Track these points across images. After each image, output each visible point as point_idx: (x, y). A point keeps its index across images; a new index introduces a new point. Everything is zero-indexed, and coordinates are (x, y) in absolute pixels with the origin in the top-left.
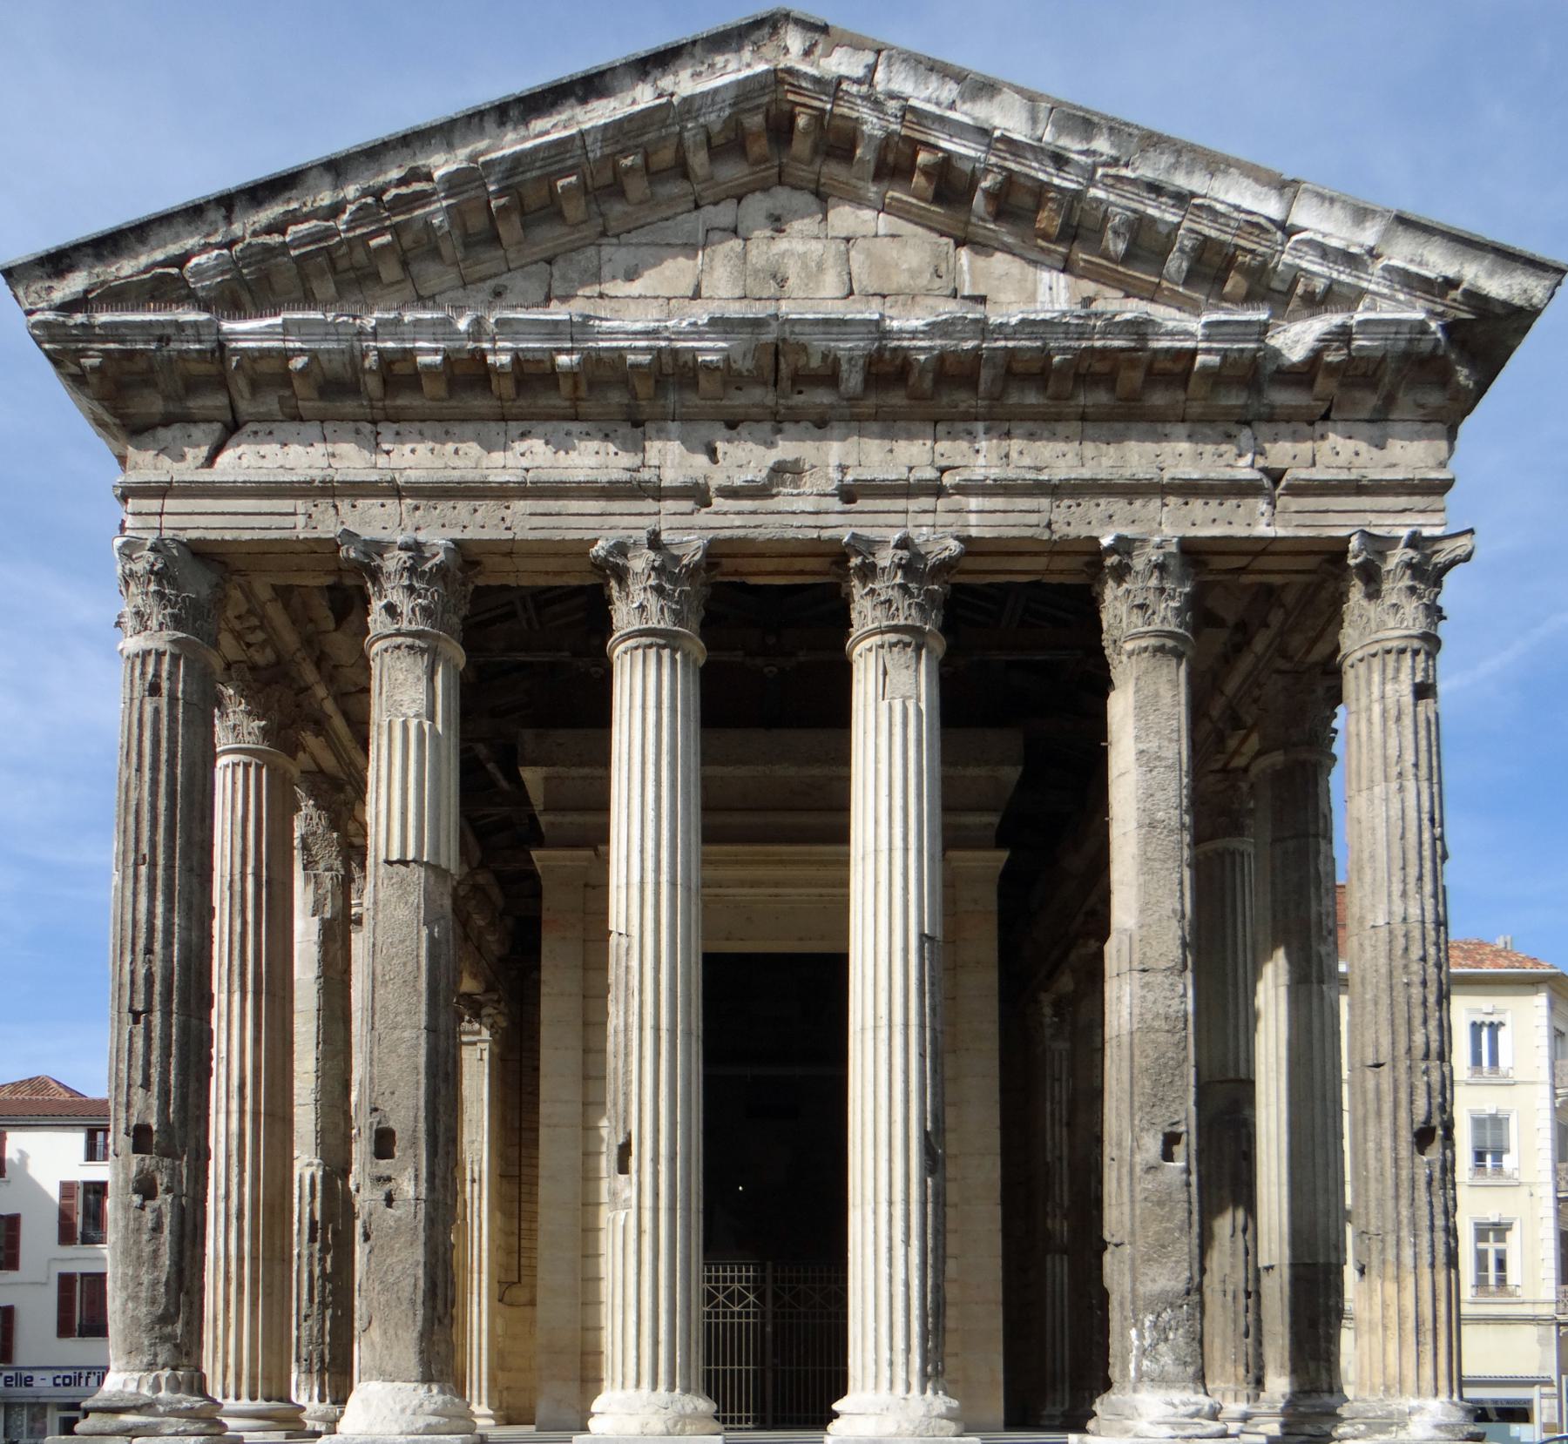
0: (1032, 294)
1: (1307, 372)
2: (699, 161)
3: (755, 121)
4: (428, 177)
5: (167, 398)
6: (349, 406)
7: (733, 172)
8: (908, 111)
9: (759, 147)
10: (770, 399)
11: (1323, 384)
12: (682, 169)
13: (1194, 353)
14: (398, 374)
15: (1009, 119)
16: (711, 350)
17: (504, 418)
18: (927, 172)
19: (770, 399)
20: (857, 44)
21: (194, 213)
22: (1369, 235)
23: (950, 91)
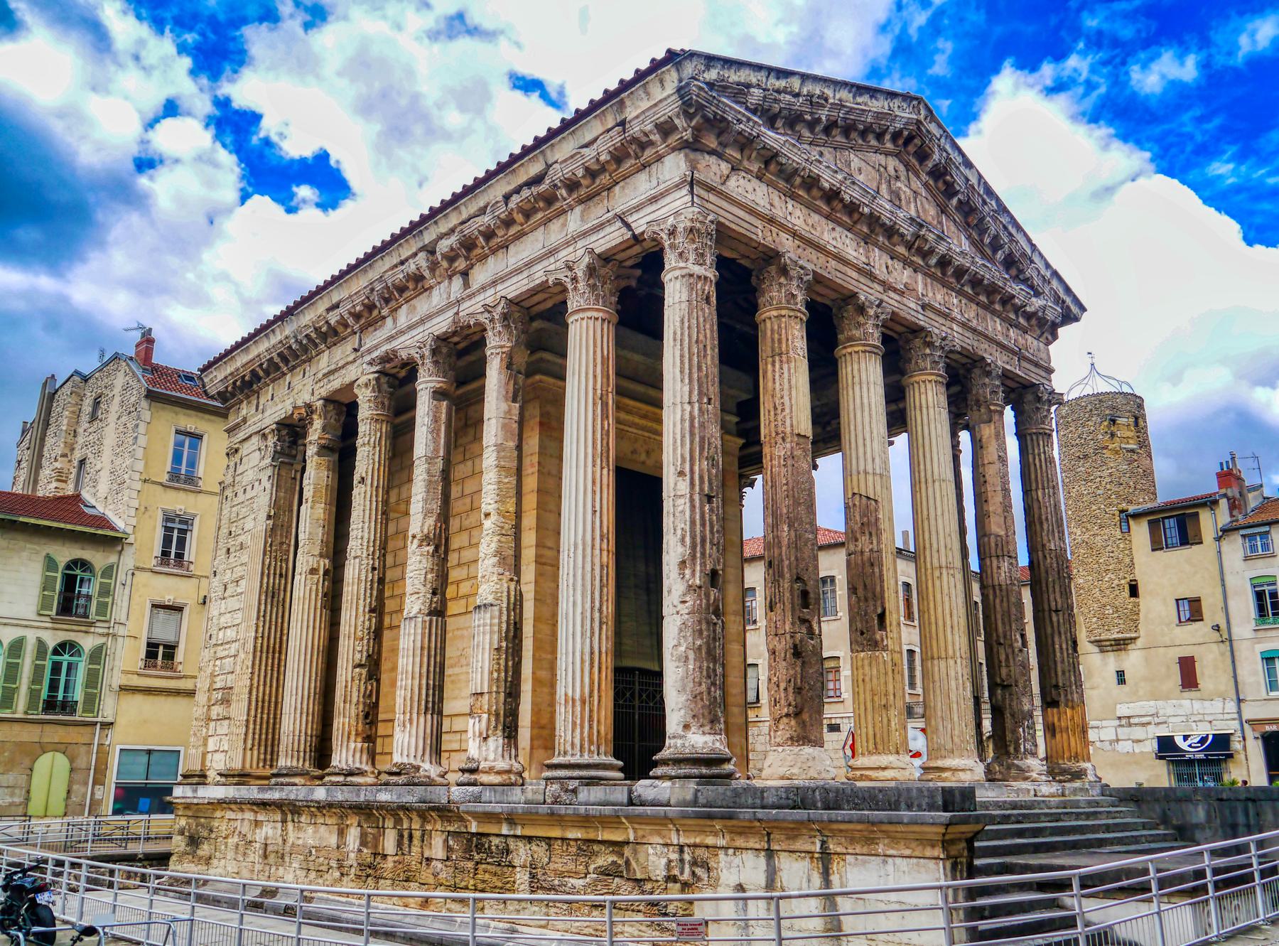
0: (959, 245)
1: (1029, 316)
2: (888, 137)
3: (906, 133)
4: (826, 100)
5: (720, 144)
6: (782, 184)
7: (889, 145)
8: (948, 158)
9: (901, 142)
10: (906, 254)
11: (1034, 322)
12: (880, 136)
13: (1014, 296)
14: (812, 183)
15: (974, 181)
16: (907, 230)
17: (827, 217)
18: (945, 182)
19: (906, 254)
20: (940, 126)
21: (758, 67)
22: (1048, 274)
23: (960, 159)
